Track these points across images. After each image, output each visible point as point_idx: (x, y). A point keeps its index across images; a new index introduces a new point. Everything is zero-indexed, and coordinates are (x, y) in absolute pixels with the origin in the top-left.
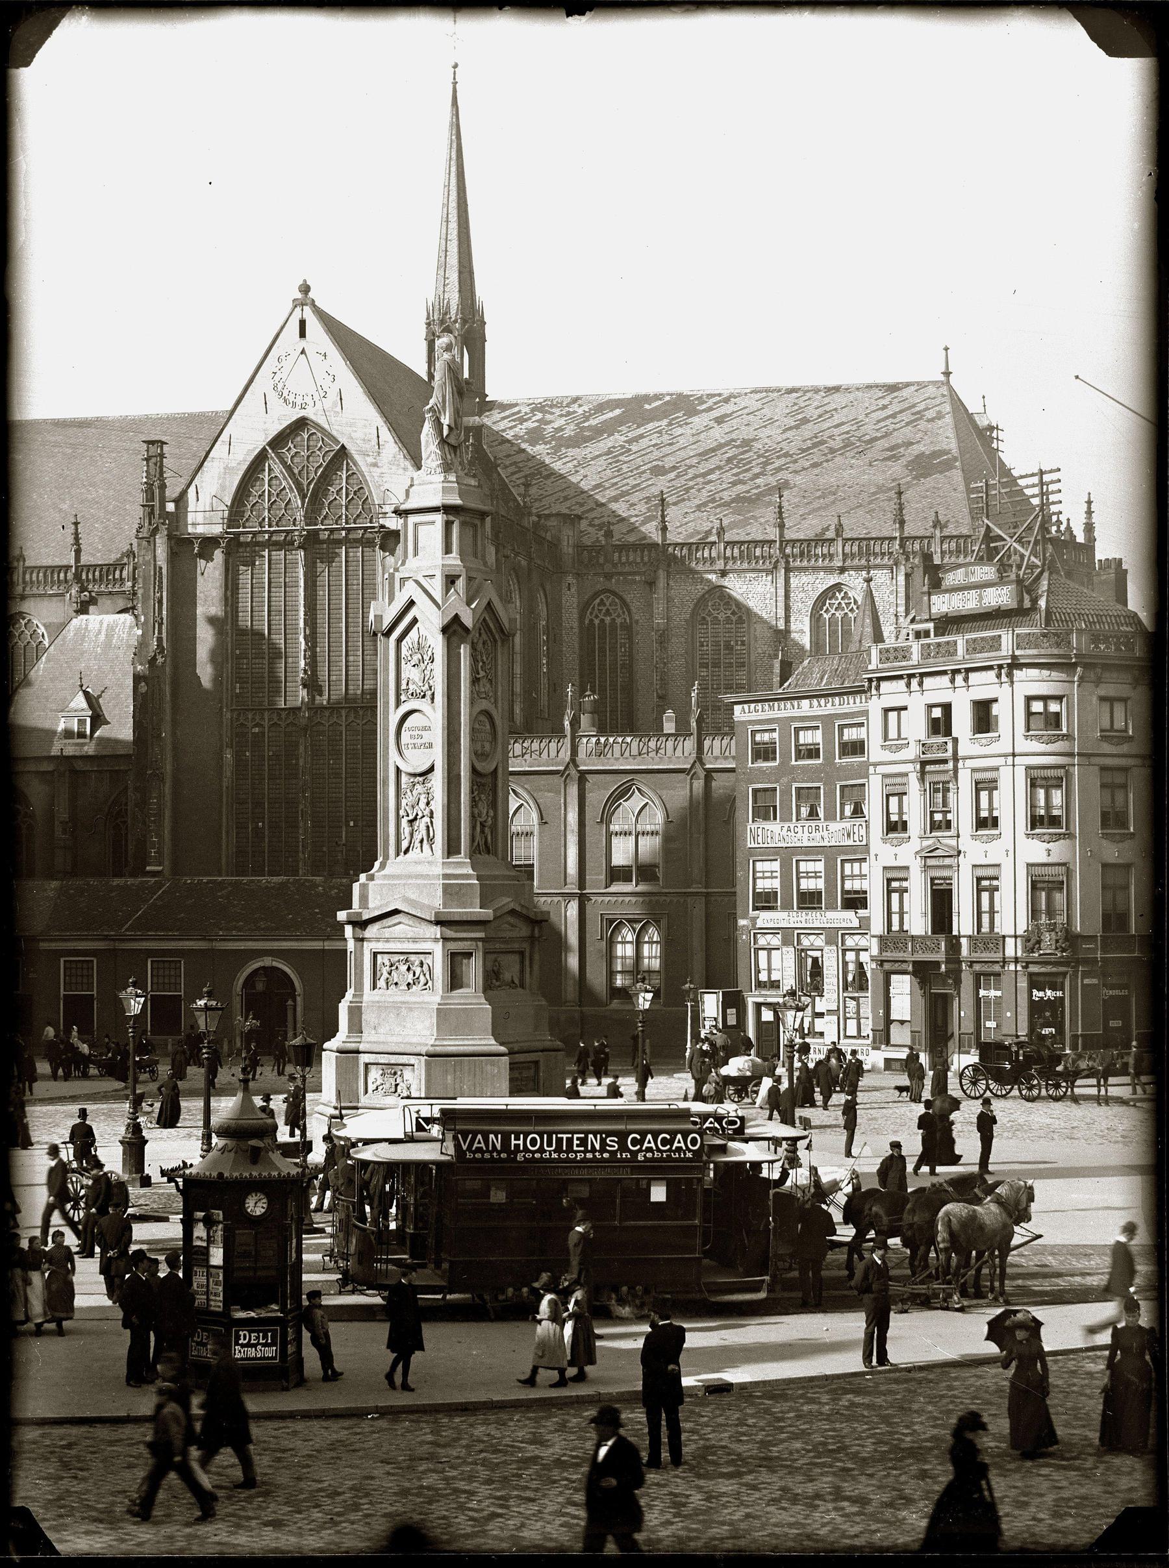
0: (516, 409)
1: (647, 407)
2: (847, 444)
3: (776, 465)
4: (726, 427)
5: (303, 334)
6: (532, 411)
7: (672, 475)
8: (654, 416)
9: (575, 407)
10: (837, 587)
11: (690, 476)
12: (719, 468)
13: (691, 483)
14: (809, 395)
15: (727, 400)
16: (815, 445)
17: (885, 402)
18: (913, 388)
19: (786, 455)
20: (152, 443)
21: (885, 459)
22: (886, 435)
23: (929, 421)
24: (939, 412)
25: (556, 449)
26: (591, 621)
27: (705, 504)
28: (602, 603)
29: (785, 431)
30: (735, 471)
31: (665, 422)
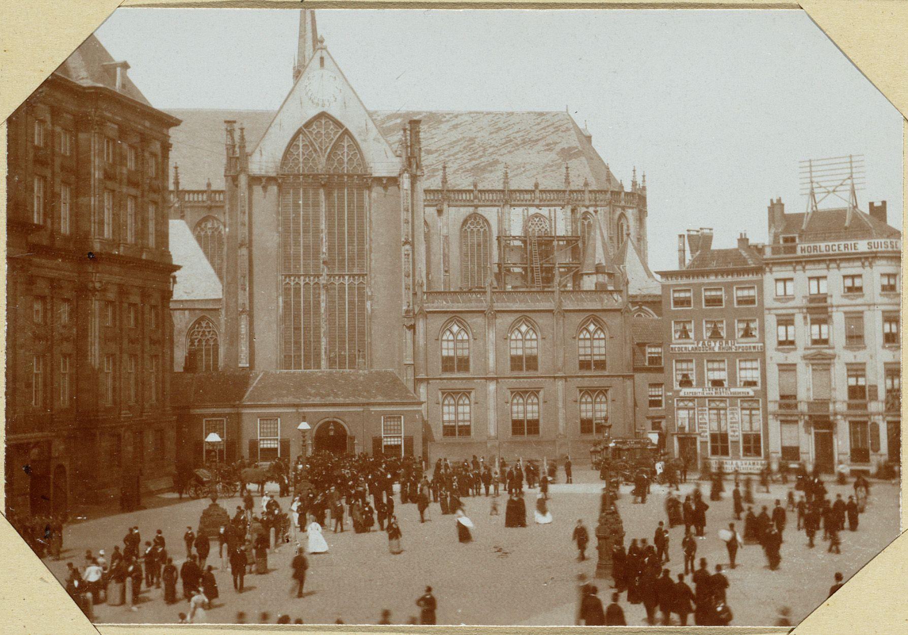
2: (524, 142)
7: (436, 155)
10: (536, 216)
11: (446, 155)
13: (447, 159)
15: (456, 117)
17: (539, 120)
21: (545, 150)
27: (457, 170)
30: (470, 153)
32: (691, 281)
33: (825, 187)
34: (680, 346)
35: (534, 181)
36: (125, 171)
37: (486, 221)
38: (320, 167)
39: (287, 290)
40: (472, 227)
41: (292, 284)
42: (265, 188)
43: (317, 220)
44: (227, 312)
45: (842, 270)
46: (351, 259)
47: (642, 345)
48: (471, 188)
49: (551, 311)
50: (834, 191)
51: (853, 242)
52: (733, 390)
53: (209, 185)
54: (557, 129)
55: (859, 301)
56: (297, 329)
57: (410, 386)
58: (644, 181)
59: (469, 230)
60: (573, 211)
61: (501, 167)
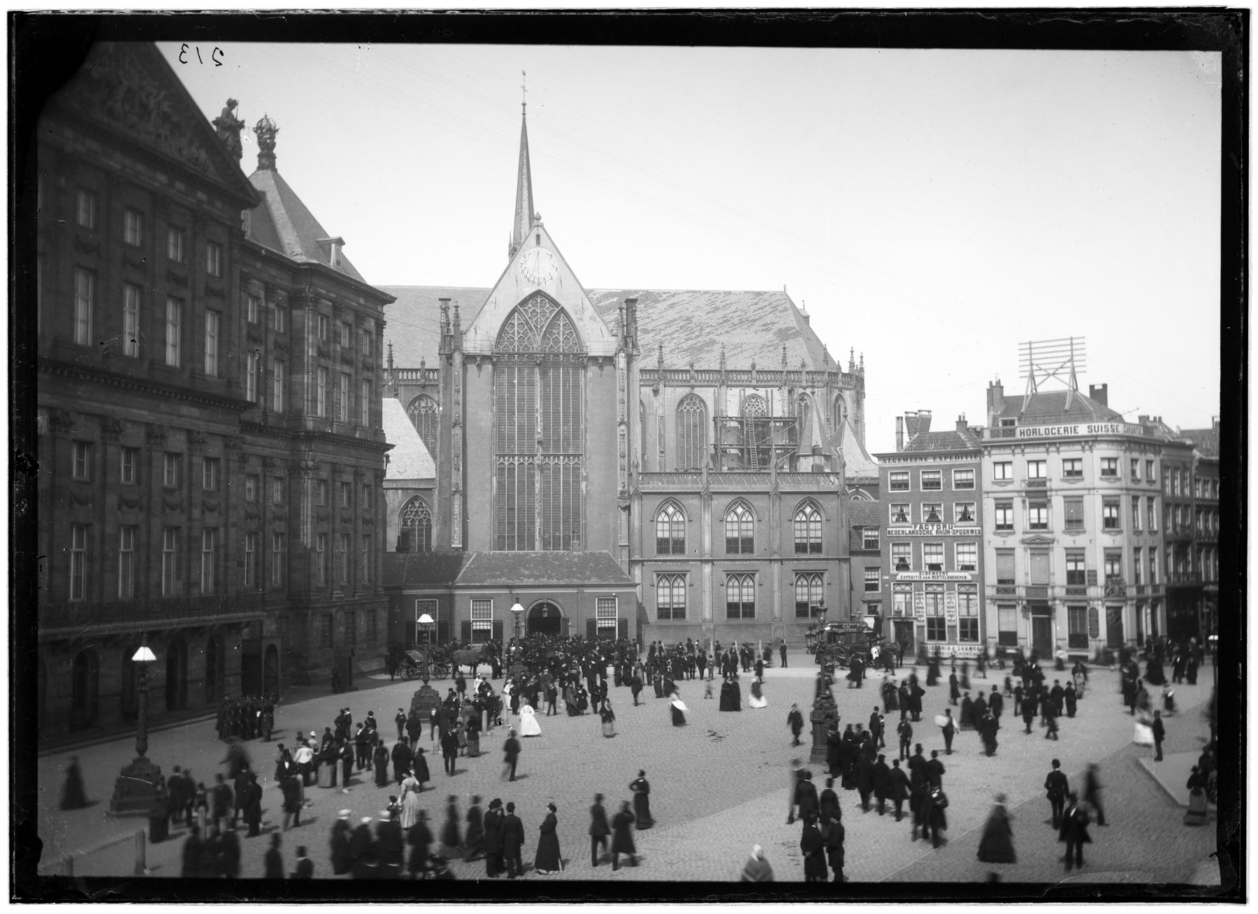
2: (741, 322)
4: (676, 309)
10: (753, 396)
11: (662, 334)
12: (677, 331)
13: (664, 339)
15: (673, 296)
16: (724, 322)
19: (711, 326)
20: (444, 300)
21: (762, 331)
22: (760, 318)
23: (780, 312)
30: (686, 333)
32: (909, 463)
33: (1045, 370)
34: (897, 529)
35: (751, 361)
36: (338, 348)
37: (703, 401)
38: (535, 346)
39: (501, 470)
40: (688, 407)
41: (506, 463)
42: (479, 367)
43: (532, 400)
44: (440, 492)
45: (992, 457)
46: (566, 439)
47: (858, 528)
48: (688, 368)
49: (767, 493)
50: (1054, 374)
51: (1073, 426)
52: (950, 574)
53: (423, 363)
54: (775, 309)
55: (1079, 485)
56: (511, 509)
57: (625, 567)
58: (862, 362)
59: (685, 411)
60: (790, 392)
61: (717, 349)
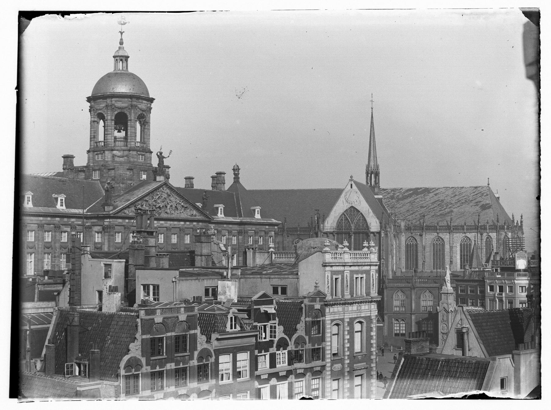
0: (387, 191)
1: (418, 191)
3: (450, 206)
4: (437, 196)
5: (351, 187)
6: (391, 191)
7: (425, 208)
8: (421, 193)
9: (401, 190)
12: (436, 207)
14: (456, 189)
15: (437, 190)
17: (474, 191)
18: (481, 188)
22: (475, 199)
23: (485, 196)
24: (487, 194)
25: (398, 201)
26: (408, 243)
27: (433, 216)
28: (410, 239)
29: (451, 198)
31: (423, 195)
40: (437, 242)
59: (435, 243)
